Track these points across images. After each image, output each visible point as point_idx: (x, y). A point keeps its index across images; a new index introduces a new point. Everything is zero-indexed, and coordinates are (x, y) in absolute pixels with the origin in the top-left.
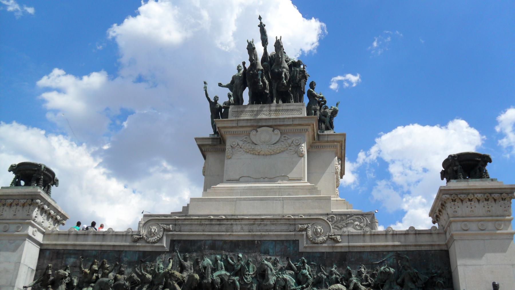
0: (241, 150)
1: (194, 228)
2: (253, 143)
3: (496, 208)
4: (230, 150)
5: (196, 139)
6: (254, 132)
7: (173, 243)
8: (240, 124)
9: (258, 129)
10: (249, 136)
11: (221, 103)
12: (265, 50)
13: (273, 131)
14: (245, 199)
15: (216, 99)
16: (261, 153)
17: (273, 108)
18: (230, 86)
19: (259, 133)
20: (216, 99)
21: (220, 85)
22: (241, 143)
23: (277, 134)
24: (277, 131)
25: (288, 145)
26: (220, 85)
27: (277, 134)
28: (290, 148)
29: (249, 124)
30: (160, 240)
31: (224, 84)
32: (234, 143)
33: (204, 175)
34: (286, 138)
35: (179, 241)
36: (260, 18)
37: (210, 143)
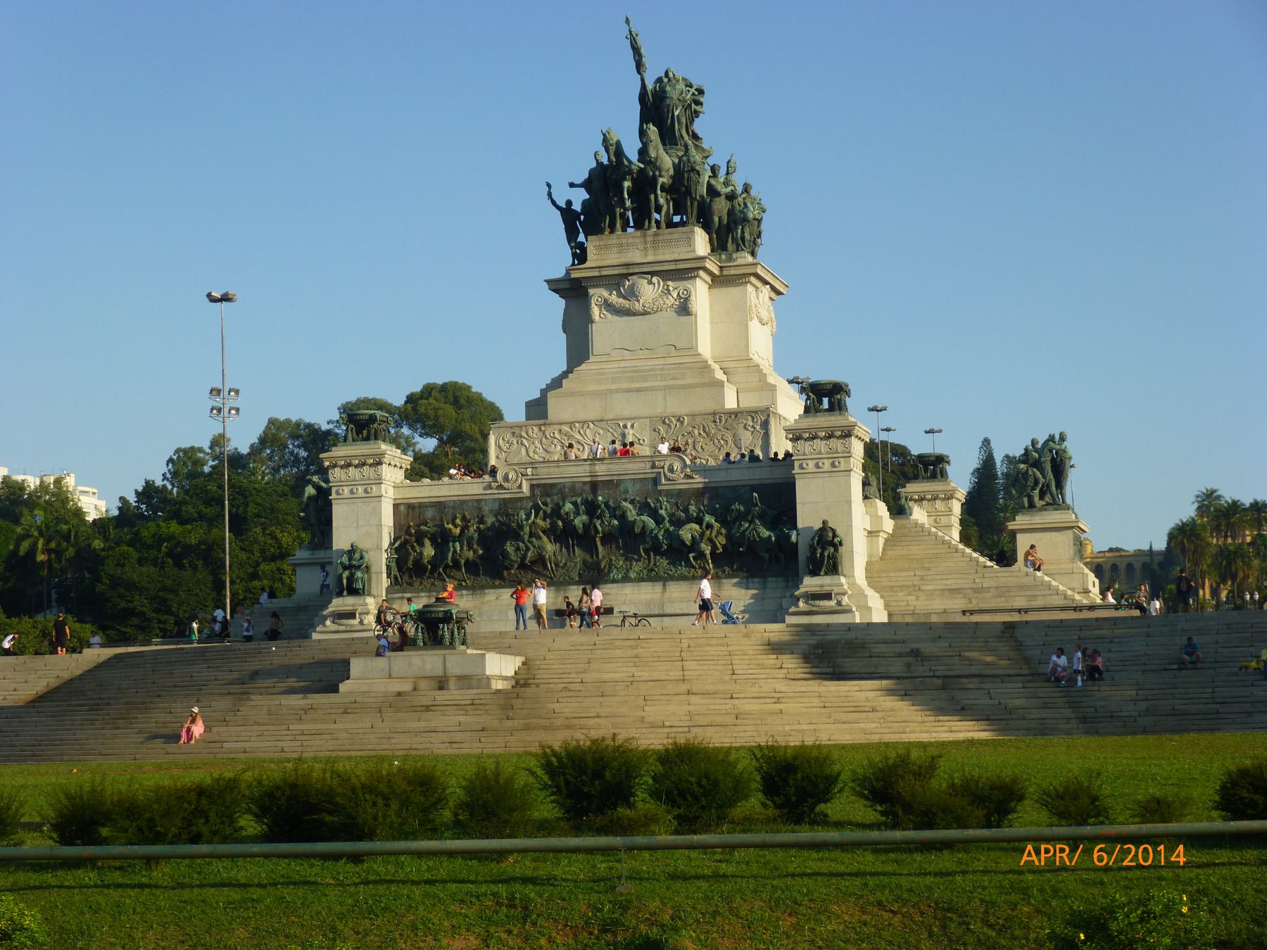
1: (552, 470)
3: (836, 444)
7: (532, 487)
8: (604, 273)
11: (577, 207)
12: (643, 80)
14: (617, 391)
15: (569, 203)
17: (649, 239)
18: (587, 185)
20: (569, 203)
21: (572, 185)
24: (655, 279)
26: (572, 185)
29: (616, 272)
30: (520, 487)
31: (579, 181)
35: (538, 485)
36: (627, 21)
37: (568, 286)
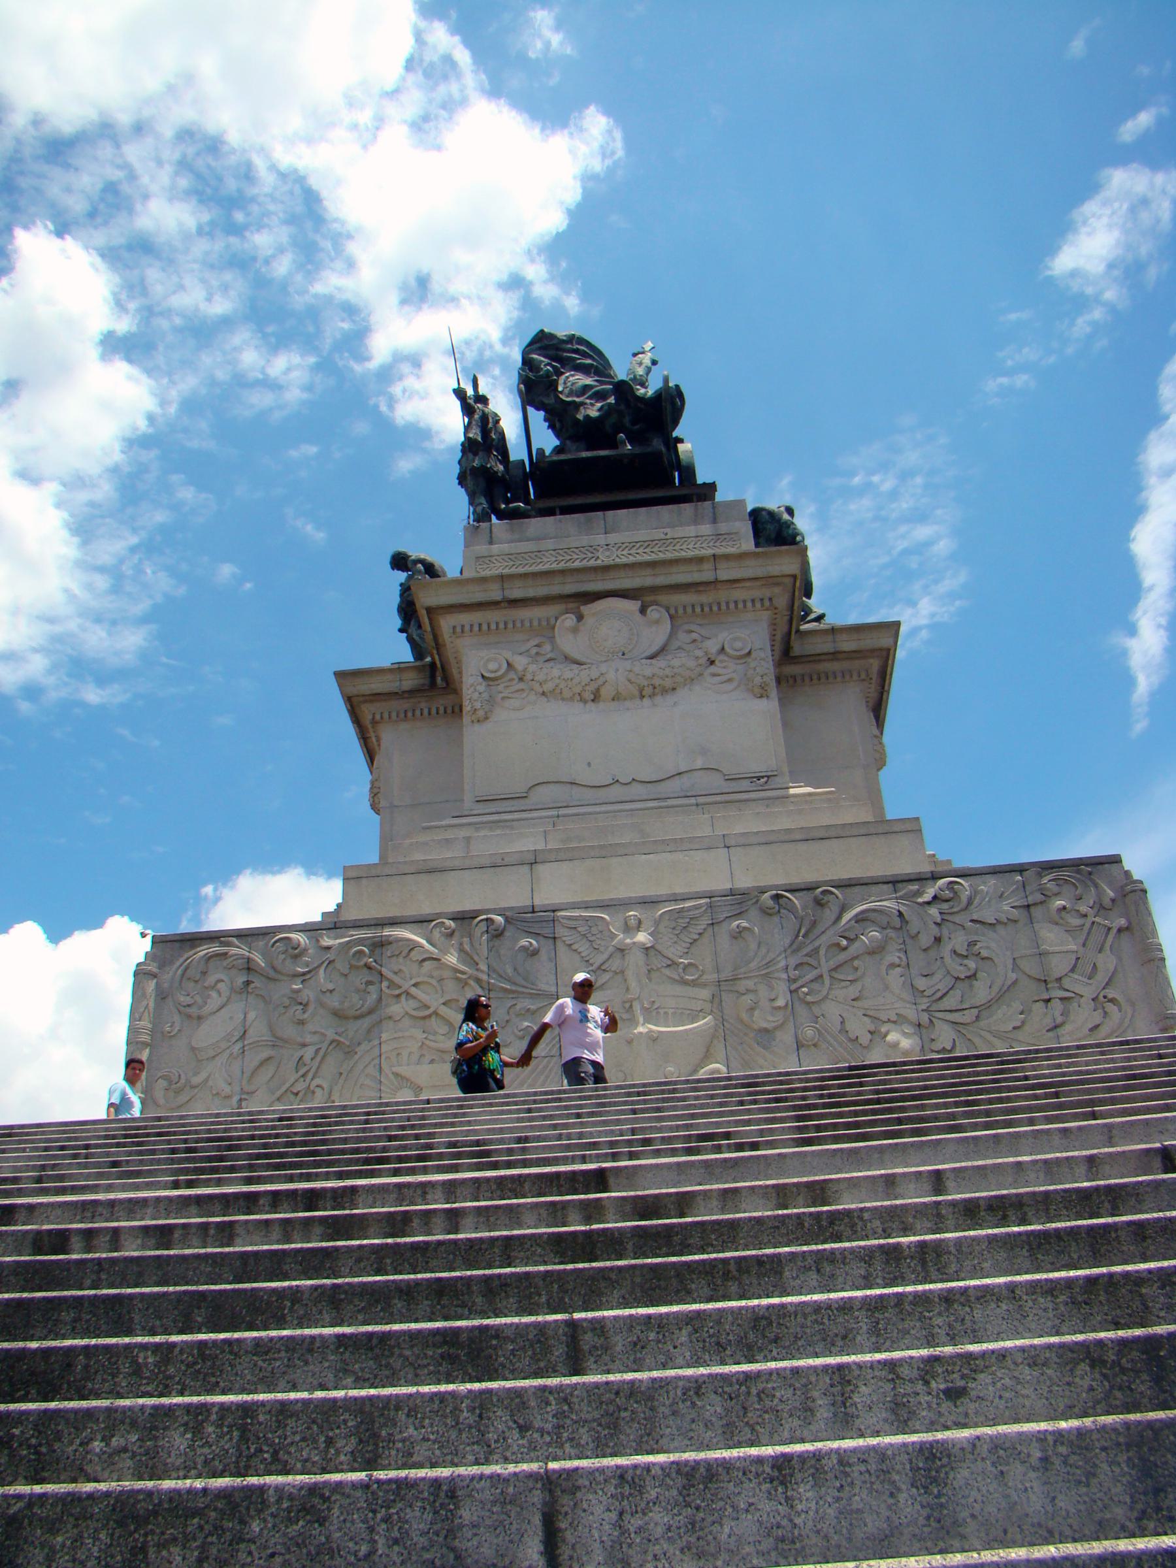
0: (521, 686)
2: (568, 659)
4: (482, 688)
5: (341, 676)
6: (570, 620)
8: (517, 593)
9: (586, 609)
10: (552, 639)
13: (643, 611)
16: (603, 691)
19: (589, 621)
22: (520, 662)
23: (657, 622)
24: (653, 613)
25: (703, 661)
27: (657, 622)
28: (712, 669)
32: (492, 666)
33: (375, 807)
34: (694, 636)
